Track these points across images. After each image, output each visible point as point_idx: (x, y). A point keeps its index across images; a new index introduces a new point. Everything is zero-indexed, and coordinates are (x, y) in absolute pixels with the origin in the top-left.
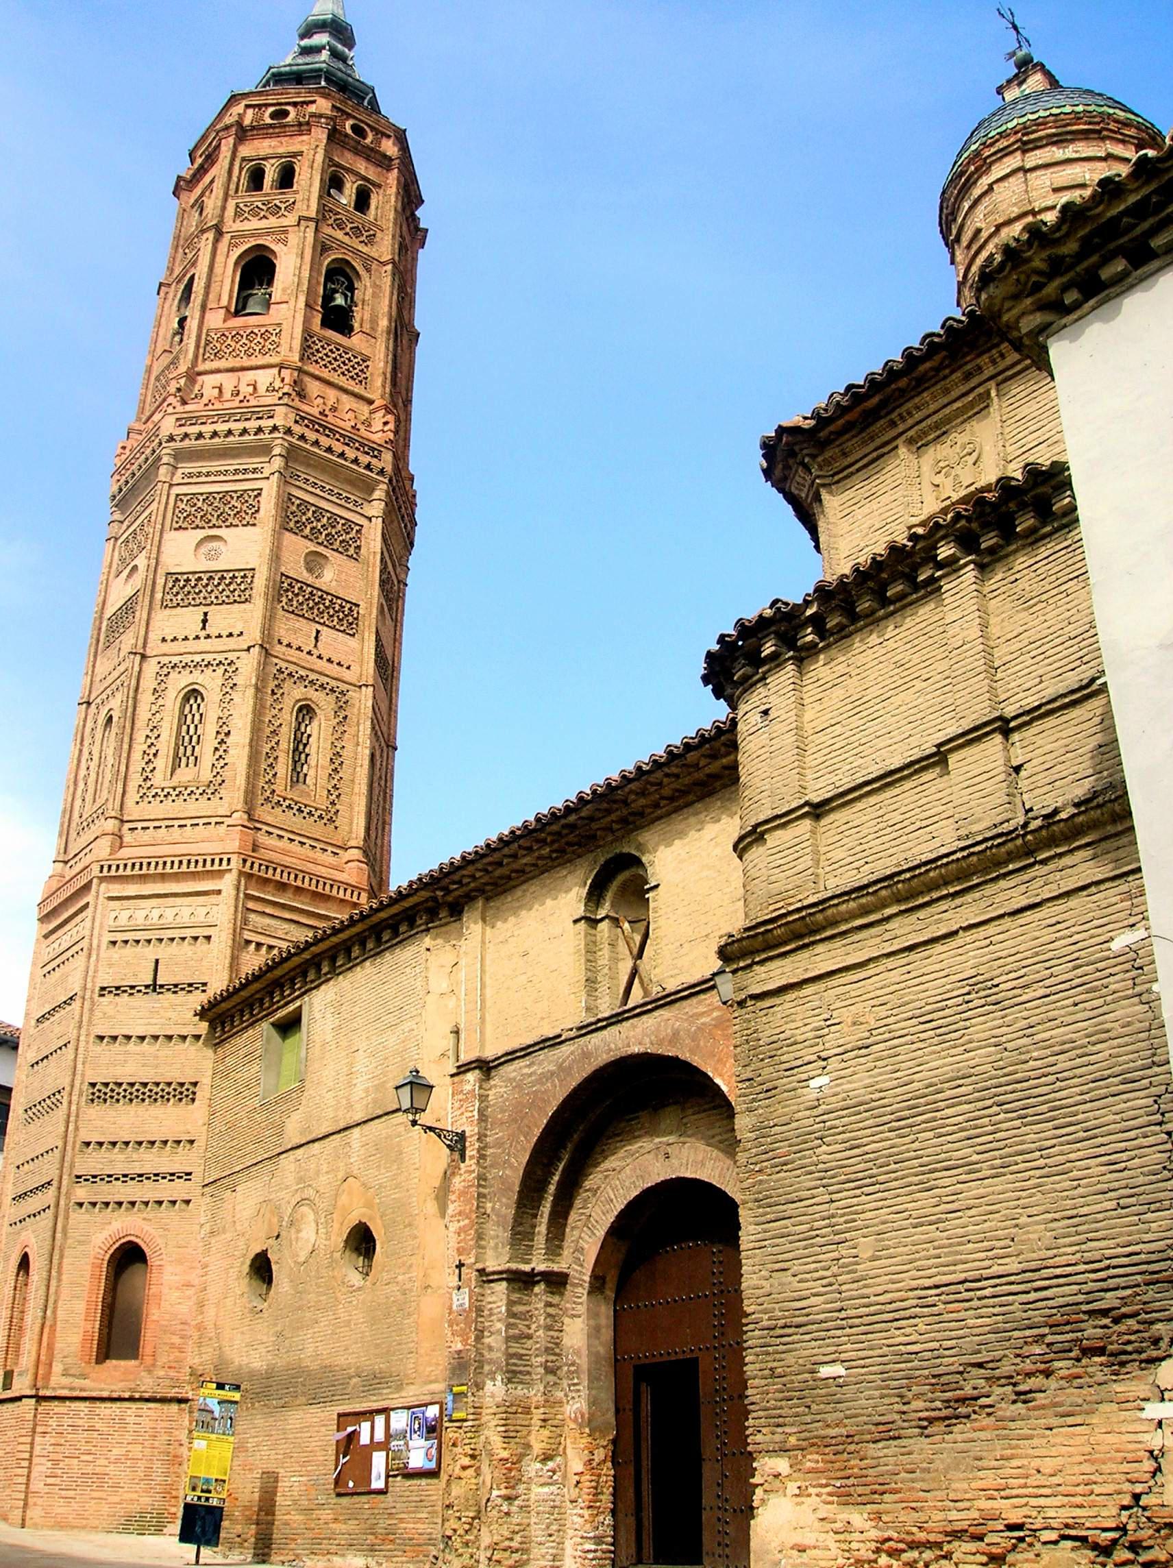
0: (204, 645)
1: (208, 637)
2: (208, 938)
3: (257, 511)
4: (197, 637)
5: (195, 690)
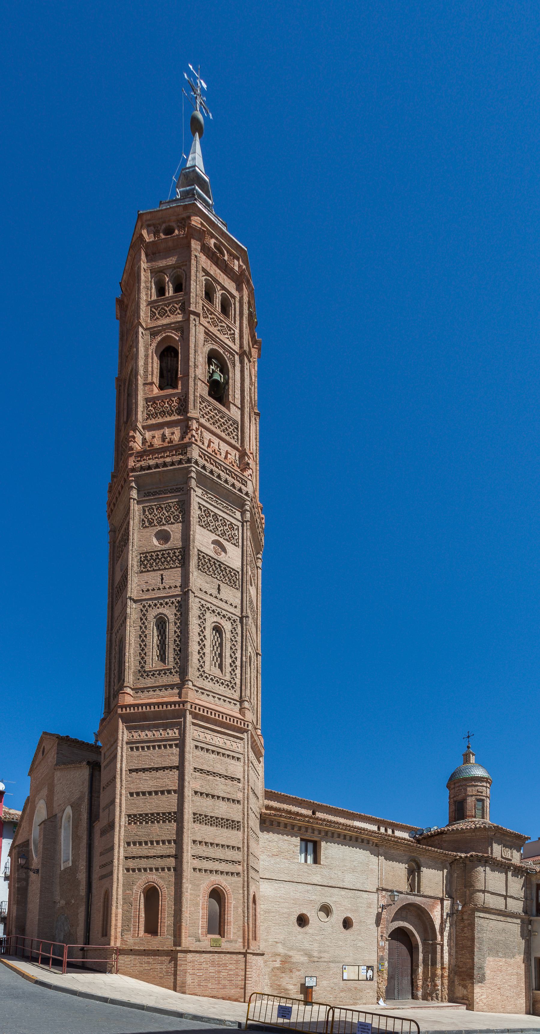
5: (161, 617)
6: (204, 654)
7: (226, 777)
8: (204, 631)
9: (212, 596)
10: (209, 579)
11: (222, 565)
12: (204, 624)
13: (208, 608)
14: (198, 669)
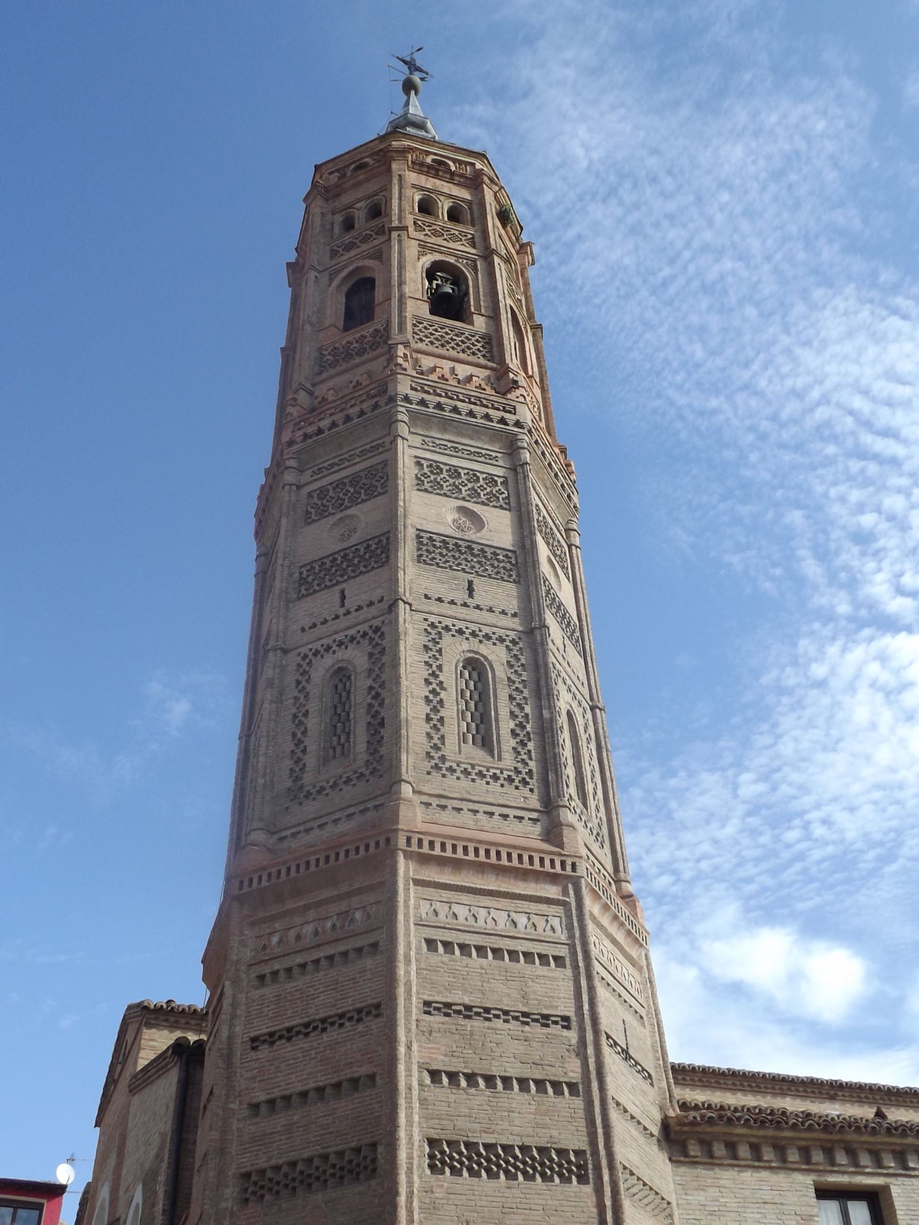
0: (344, 622)
2: (375, 945)
4: (337, 617)
6: (441, 720)
7: (525, 1017)
8: (438, 672)
9: (455, 604)
11: (474, 546)
12: (437, 659)
13: (447, 629)
14: (428, 753)
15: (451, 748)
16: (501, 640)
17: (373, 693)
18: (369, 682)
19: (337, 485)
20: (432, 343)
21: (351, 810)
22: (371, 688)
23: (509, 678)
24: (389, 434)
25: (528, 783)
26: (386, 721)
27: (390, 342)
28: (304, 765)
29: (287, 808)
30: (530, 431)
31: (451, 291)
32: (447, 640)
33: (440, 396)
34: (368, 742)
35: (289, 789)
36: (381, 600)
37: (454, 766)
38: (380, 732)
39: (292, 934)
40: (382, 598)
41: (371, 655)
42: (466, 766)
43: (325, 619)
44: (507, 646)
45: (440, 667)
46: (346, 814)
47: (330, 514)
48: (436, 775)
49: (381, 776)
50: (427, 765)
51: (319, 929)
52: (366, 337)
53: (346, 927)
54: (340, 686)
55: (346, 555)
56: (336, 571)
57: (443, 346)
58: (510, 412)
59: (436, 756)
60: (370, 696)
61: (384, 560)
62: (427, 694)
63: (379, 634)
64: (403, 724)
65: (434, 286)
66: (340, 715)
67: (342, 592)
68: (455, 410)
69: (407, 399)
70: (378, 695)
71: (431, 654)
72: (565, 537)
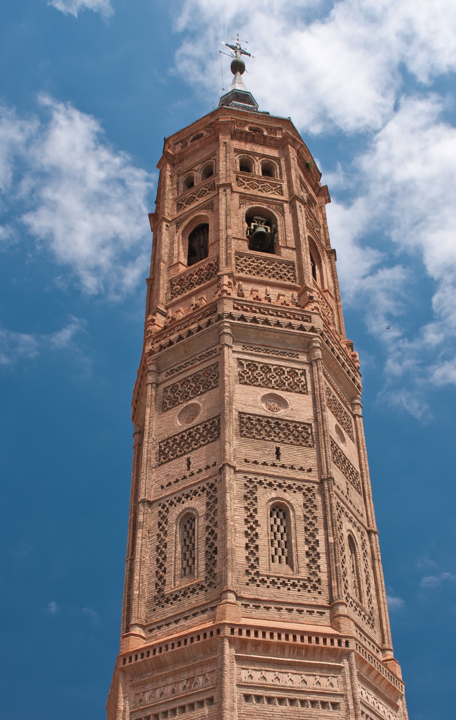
1: (192, 474)
3: (217, 378)
4: (185, 477)
5: (188, 514)
6: (257, 547)
8: (254, 514)
10: (259, 444)
12: (254, 505)
13: (261, 483)
14: (247, 571)
15: (263, 567)
16: (300, 489)
17: (210, 531)
18: (207, 523)
19: (184, 383)
20: (250, 272)
21: (196, 611)
22: (208, 527)
23: (305, 516)
24: (219, 343)
25: (317, 588)
26: (218, 549)
27: (218, 274)
28: (165, 581)
29: (154, 610)
30: (322, 334)
31: (264, 230)
32: (260, 491)
33: (255, 312)
34: (207, 564)
35: (155, 597)
36: (214, 465)
37: (265, 578)
38: (214, 557)
39: (158, 692)
40: (215, 463)
41: (208, 504)
42: (273, 578)
43: (177, 479)
44: (304, 493)
45: (255, 511)
46: (193, 613)
47: (179, 404)
48: (253, 586)
49: (215, 587)
50: (246, 579)
51: (175, 689)
52: (202, 270)
53: (192, 687)
54: (188, 526)
55: (190, 433)
56: (184, 444)
57: (258, 273)
58: (307, 321)
59: (253, 572)
60: (207, 533)
61: (216, 435)
62: (247, 529)
63: (213, 489)
64: (229, 552)
65: (252, 228)
66: (188, 546)
67: (188, 460)
68: (266, 322)
69: (231, 316)
70: (212, 532)
71: (249, 502)
72: (351, 409)
